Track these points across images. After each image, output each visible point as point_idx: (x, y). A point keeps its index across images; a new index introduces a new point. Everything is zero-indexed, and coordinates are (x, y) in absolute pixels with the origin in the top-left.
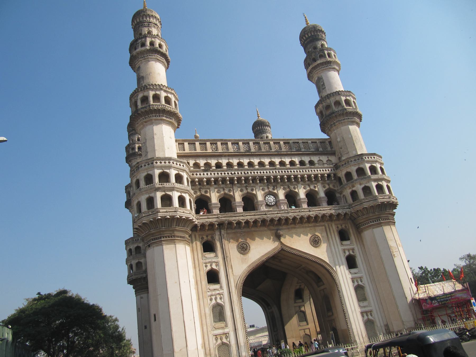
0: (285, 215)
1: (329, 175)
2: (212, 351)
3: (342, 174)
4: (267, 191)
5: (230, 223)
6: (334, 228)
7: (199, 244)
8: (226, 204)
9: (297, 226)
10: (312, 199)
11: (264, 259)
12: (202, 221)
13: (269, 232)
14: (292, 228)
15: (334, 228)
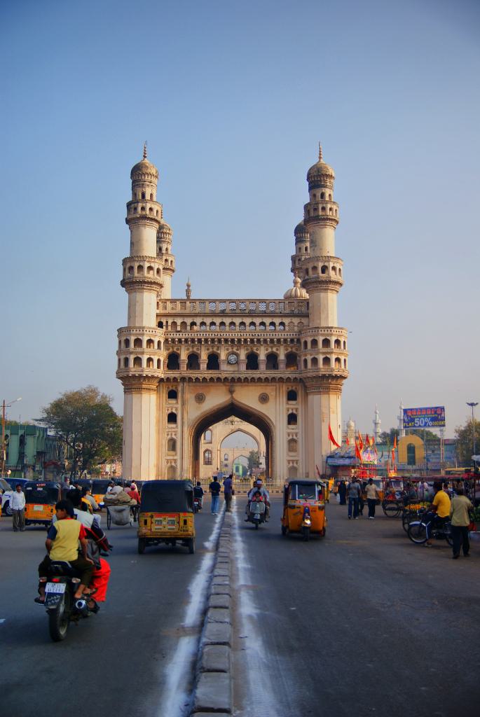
0: (238, 376)
1: (292, 340)
2: (163, 470)
3: (303, 341)
4: (230, 350)
5: (190, 378)
6: (284, 389)
7: (165, 391)
8: (193, 360)
9: (250, 384)
10: (272, 360)
11: (215, 408)
12: (168, 376)
13: (224, 387)
14: (245, 386)
15: (284, 389)
